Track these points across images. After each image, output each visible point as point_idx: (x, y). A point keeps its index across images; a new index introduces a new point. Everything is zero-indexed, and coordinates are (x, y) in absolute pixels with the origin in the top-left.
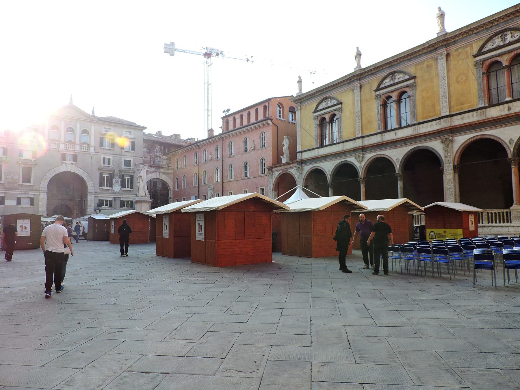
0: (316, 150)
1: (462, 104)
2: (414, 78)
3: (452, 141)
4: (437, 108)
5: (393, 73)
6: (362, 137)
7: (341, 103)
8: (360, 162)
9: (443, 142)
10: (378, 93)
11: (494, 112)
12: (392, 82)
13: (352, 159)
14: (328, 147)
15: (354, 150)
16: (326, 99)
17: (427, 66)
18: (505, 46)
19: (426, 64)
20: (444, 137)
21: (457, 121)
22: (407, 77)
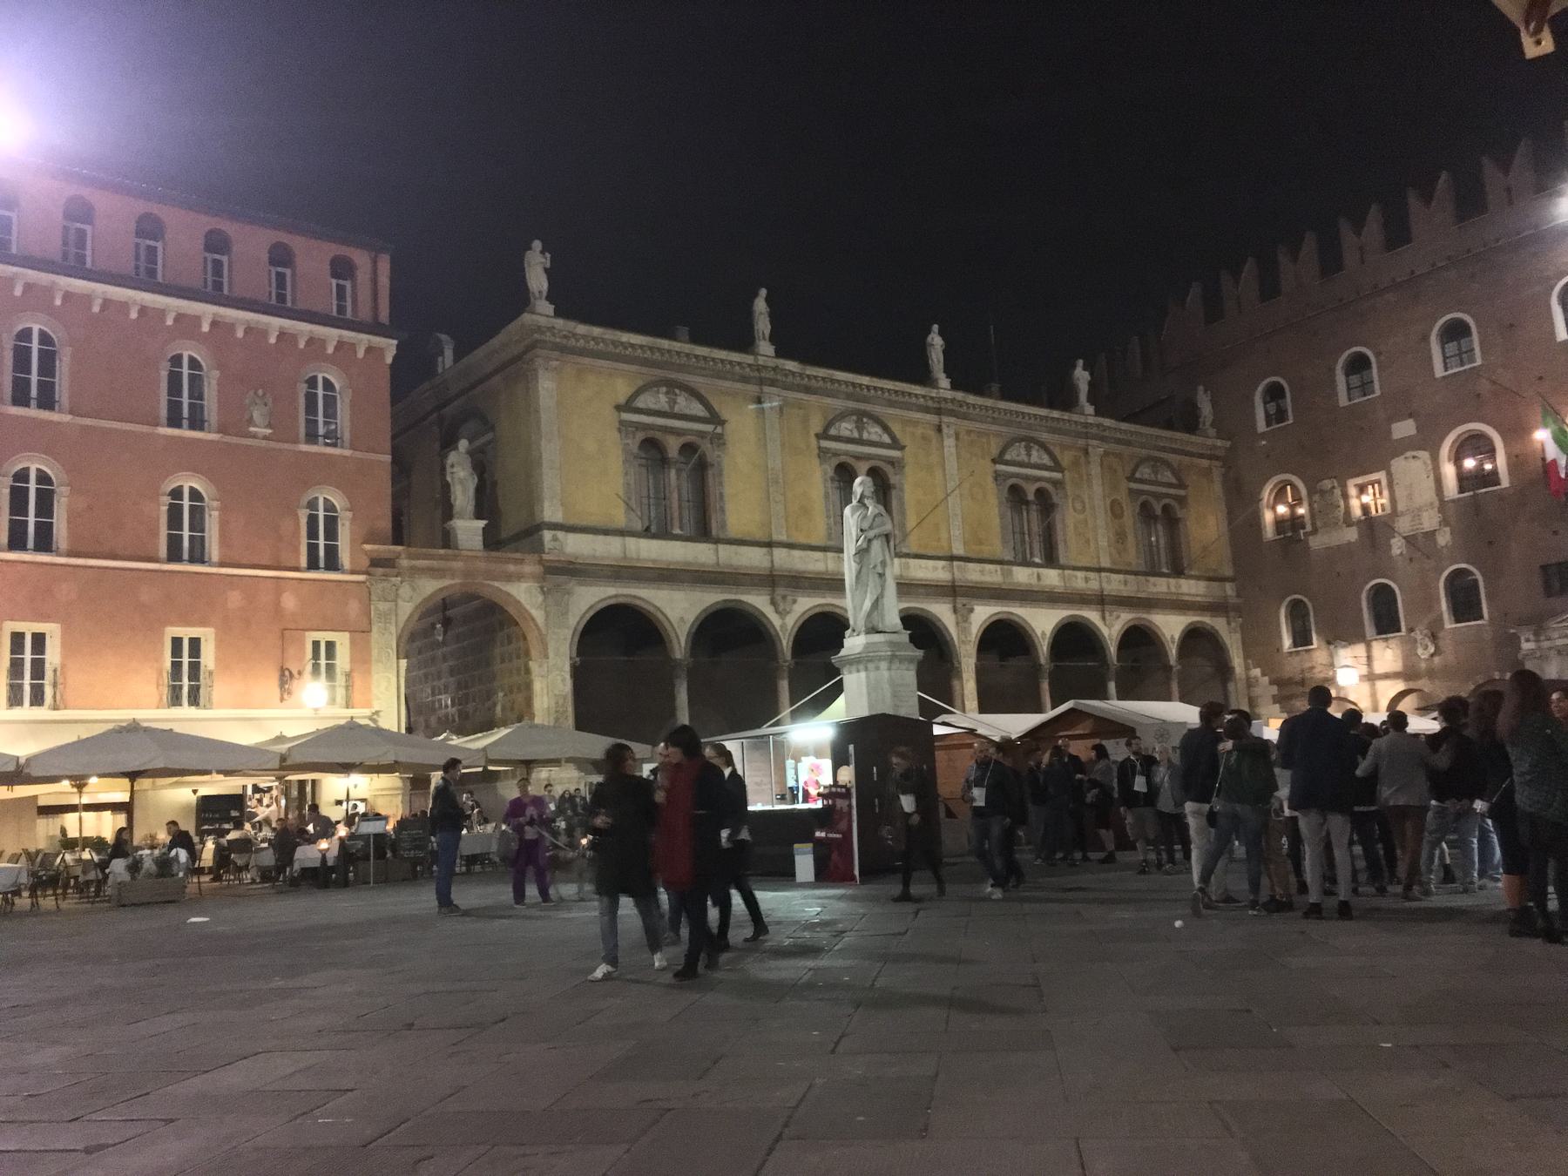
0: (631, 542)
1: (981, 543)
2: (902, 448)
3: (972, 610)
4: (944, 535)
5: (861, 415)
6: (790, 546)
7: (722, 423)
8: (782, 614)
9: (955, 611)
10: (825, 444)
11: (1022, 576)
12: (856, 435)
13: (758, 601)
14: (678, 543)
15: (771, 580)
16: (672, 386)
17: (924, 438)
18: (1021, 464)
19: (919, 431)
20: (960, 601)
21: (974, 574)
22: (886, 439)
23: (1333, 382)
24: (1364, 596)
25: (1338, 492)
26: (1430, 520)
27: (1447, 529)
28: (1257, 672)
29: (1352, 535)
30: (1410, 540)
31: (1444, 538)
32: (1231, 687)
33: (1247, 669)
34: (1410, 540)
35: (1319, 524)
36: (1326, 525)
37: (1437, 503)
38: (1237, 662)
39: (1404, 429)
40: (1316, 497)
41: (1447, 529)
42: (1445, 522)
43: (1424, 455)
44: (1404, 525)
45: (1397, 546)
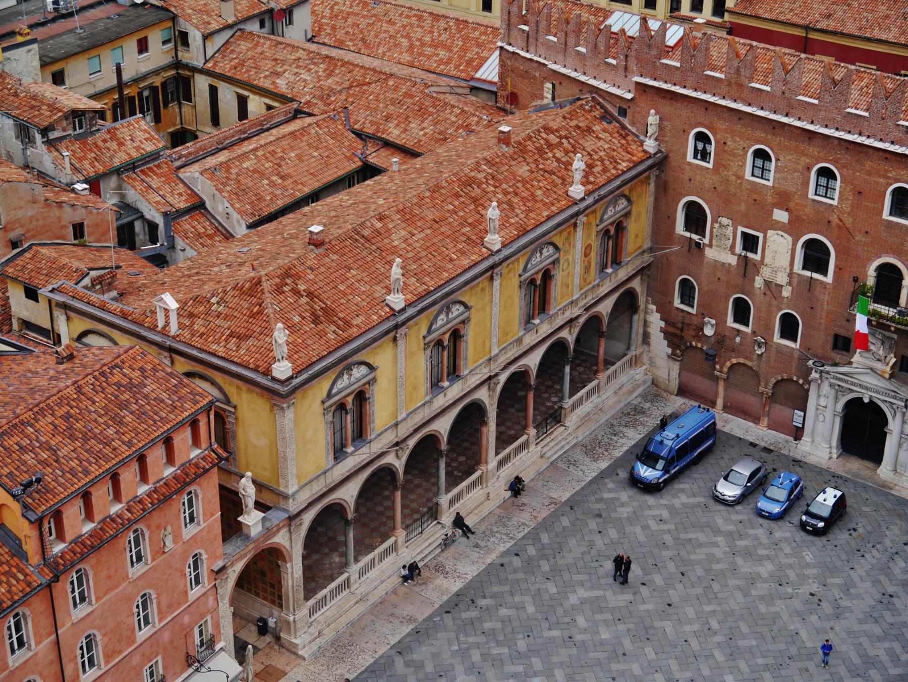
23: (745, 160)
24: (731, 300)
25: (730, 229)
26: (782, 278)
27: (790, 288)
28: (654, 308)
29: (733, 260)
30: (767, 283)
31: (786, 292)
32: (635, 317)
33: (647, 302)
34: (767, 283)
35: (714, 242)
36: (718, 246)
37: (788, 270)
38: (642, 300)
39: (781, 216)
40: (716, 225)
41: (790, 288)
42: (790, 283)
43: (790, 239)
44: (766, 272)
45: (759, 282)
